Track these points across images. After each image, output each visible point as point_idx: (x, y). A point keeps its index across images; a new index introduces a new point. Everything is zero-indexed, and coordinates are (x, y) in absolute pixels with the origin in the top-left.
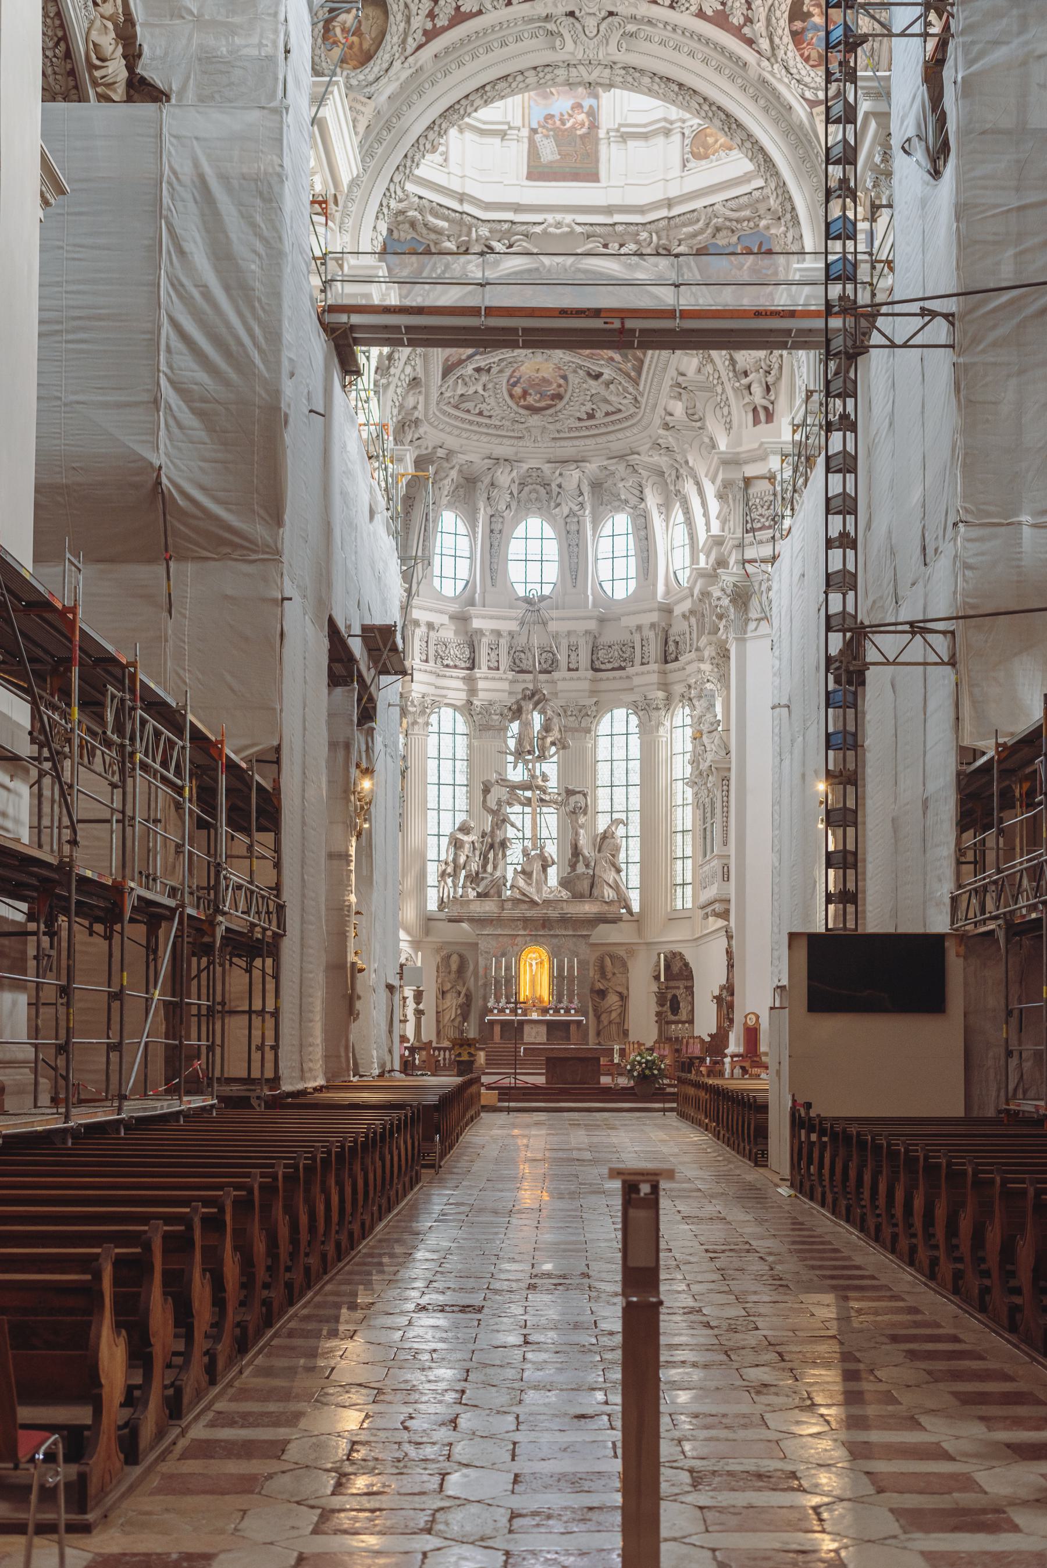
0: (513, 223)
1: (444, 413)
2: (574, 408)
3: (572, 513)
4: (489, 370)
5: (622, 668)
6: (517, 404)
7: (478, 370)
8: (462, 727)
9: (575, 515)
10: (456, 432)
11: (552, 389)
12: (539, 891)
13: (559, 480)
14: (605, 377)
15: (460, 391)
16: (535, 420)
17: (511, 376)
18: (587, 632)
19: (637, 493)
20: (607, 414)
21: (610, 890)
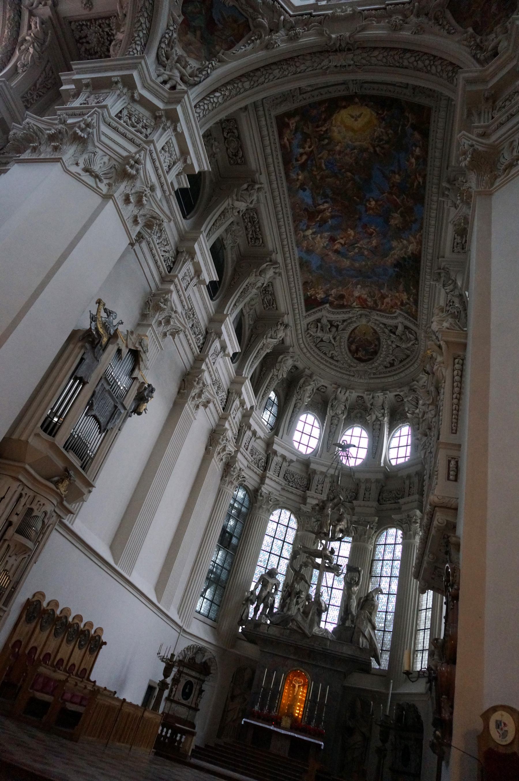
0: (310, 14)
1: (311, 348)
2: (383, 357)
3: (377, 419)
4: (337, 327)
5: (396, 503)
6: (353, 356)
7: (330, 322)
8: (294, 524)
9: (379, 420)
10: (317, 363)
11: (371, 349)
12: (311, 626)
13: (372, 400)
14: (400, 328)
15: (320, 334)
16: (361, 366)
17: (350, 337)
18: (377, 481)
19: (414, 403)
20: (401, 361)
21: (365, 640)
